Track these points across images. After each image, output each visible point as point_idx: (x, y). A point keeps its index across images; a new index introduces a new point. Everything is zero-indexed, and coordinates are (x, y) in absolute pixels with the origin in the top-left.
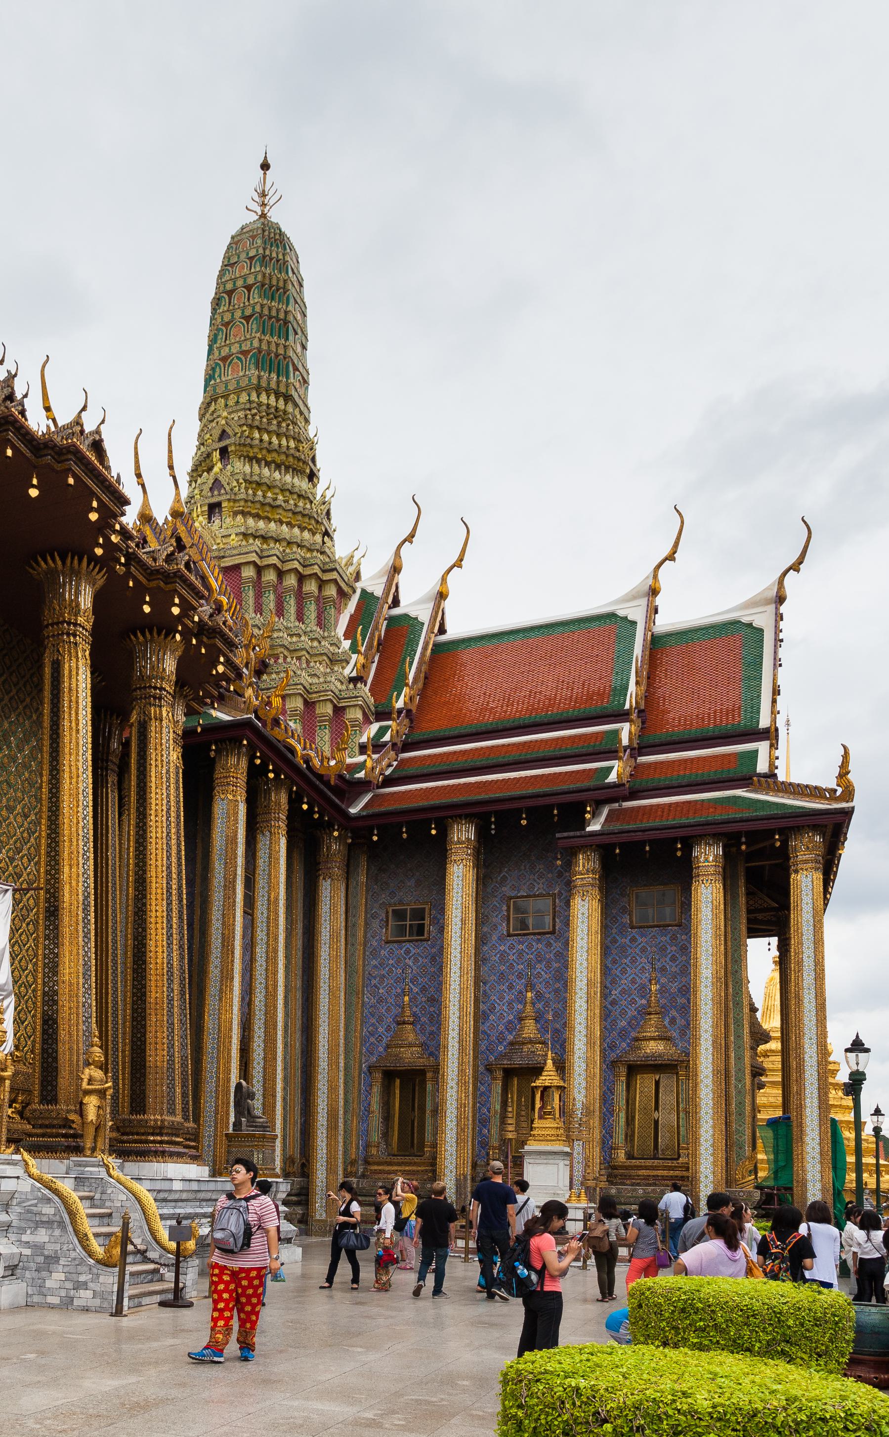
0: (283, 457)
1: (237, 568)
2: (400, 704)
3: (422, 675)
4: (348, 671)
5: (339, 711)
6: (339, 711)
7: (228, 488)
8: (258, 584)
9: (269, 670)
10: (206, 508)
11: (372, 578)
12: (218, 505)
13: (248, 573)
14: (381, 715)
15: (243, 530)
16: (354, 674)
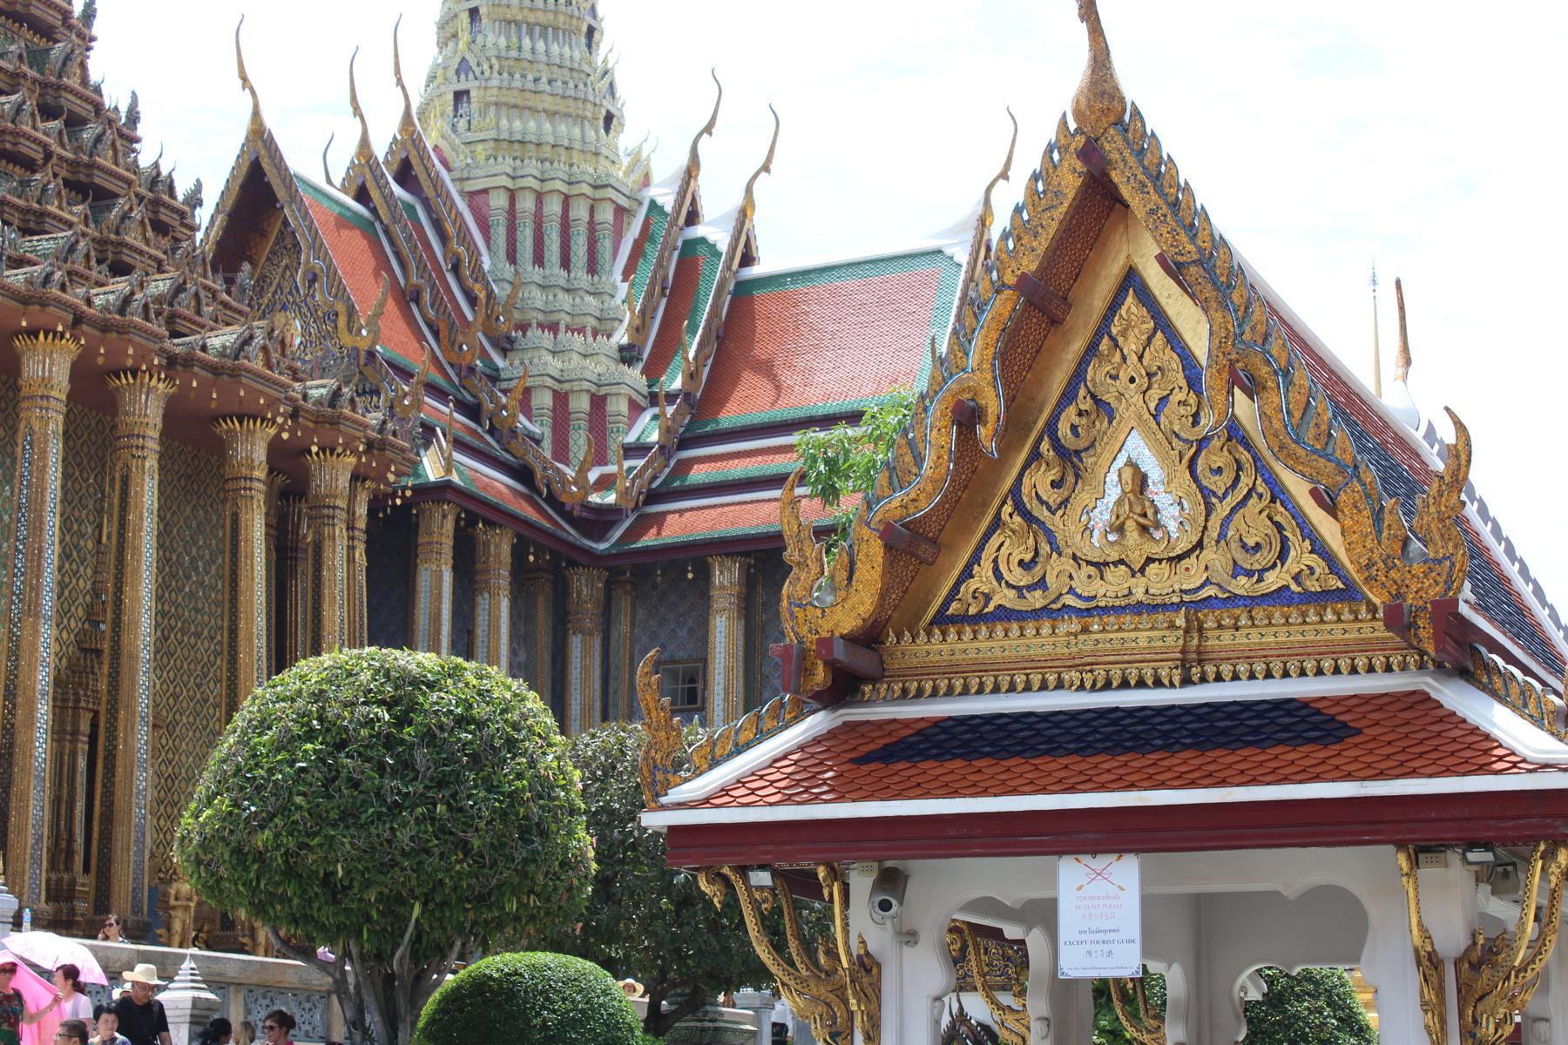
0: (551, 16)
1: (485, 191)
2: (677, 384)
3: (714, 334)
4: (621, 337)
5: (598, 402)
6: (598, 402)
7: (478, 71)
8: (512, 213)
9: (516, 346)
10: (450, 97)
11: (662, 184)
12: (467, 92)
13: (499, 201)
14: (653, 399)
15: (492, 134)
16: (625, 340)
